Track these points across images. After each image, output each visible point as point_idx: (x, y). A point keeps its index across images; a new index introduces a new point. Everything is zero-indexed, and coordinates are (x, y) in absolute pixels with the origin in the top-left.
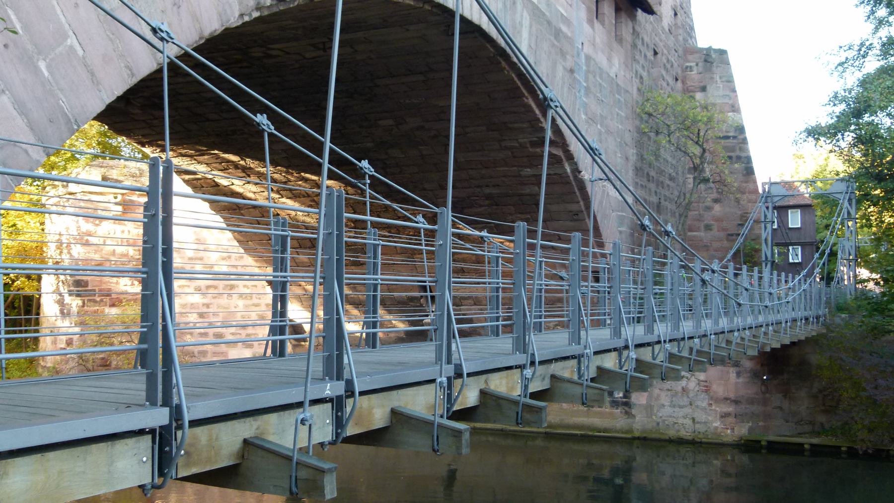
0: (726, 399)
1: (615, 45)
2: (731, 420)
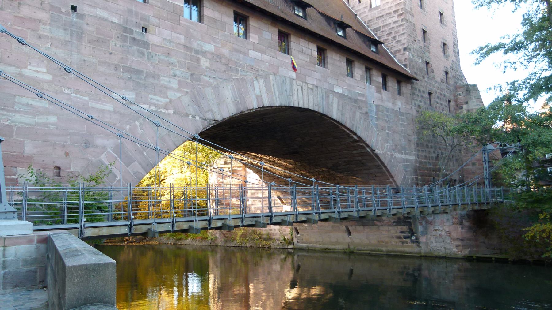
0: (458, 239)
1: (398, 96)
2: (460, 248)
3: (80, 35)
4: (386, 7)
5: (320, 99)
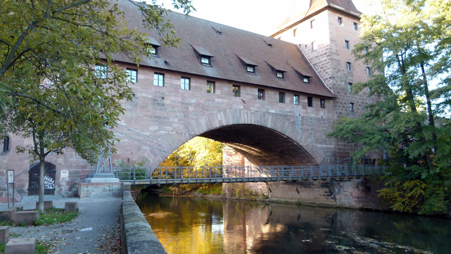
0: (356, 197)
2: (357, 202)
3: (136, 106)
4: (320, 51)
5: (259, 118)
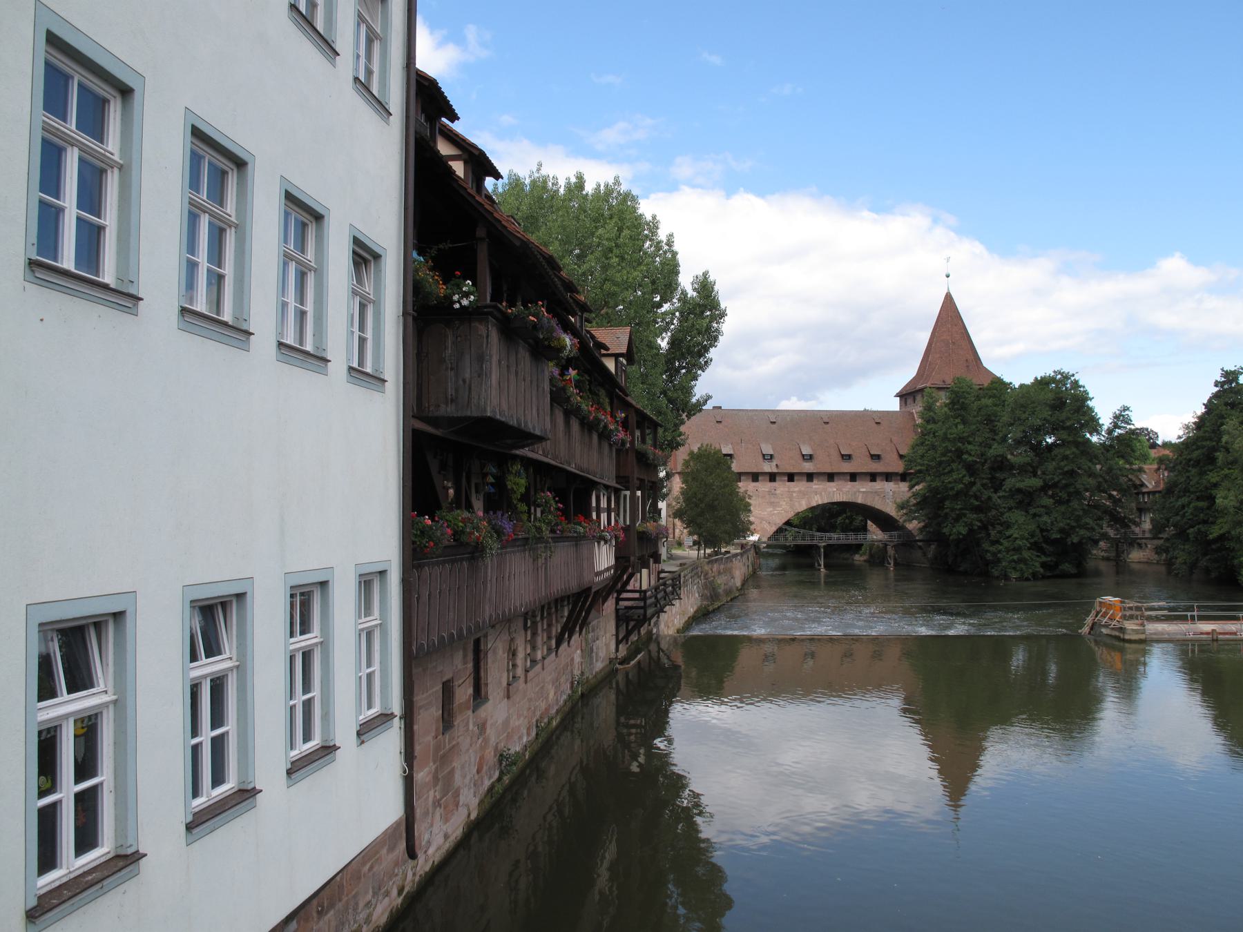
3: (759, 496)
